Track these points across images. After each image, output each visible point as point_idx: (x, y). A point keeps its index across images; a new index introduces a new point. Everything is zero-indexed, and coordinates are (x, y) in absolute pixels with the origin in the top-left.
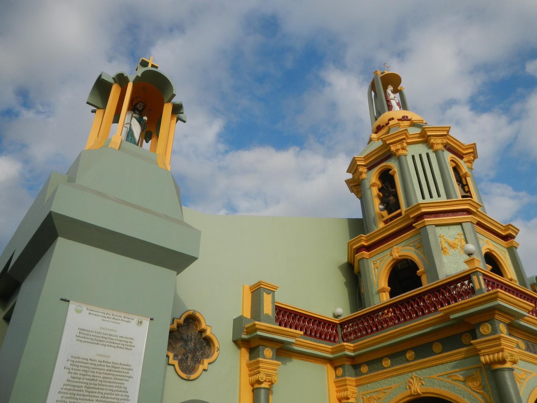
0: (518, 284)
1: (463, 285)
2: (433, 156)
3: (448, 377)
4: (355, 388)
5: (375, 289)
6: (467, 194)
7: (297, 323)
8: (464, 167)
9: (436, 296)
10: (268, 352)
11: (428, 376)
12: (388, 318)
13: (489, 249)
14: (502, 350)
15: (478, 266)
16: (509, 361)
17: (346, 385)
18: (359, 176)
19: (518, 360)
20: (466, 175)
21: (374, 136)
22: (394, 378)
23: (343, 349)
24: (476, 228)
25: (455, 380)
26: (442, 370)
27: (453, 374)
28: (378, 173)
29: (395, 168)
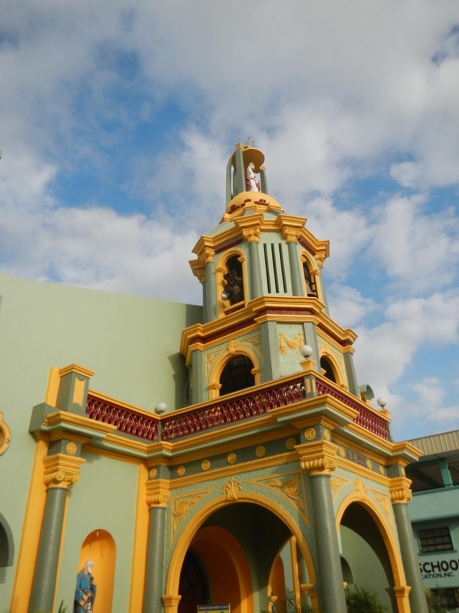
0: (348, 391)
1: (295, 387)
2: (285, 248)
3: (267, 482)
4: (168, 491)
5: (205, 385)
6: (313, 293)
7: (111, 416)
8: (315, 265)
9: (267, 398)
10: (72, 447)
11: (246, 481)
12: (214, 417)
13: (326, 353)
14: (322, 457)
15: (313, 369)
16: (328, 468)
17: (158, 488)
18: (205, 258)
19: (336, 467)
20: (315, 273)
21: (227, 216)
22: (212, 482)
23: (161, 448)
24: (316, 329)
25: (273, 486)
26: (262, 475)
27: (272, 479)
28: (226, 258)
29: (245, 255)
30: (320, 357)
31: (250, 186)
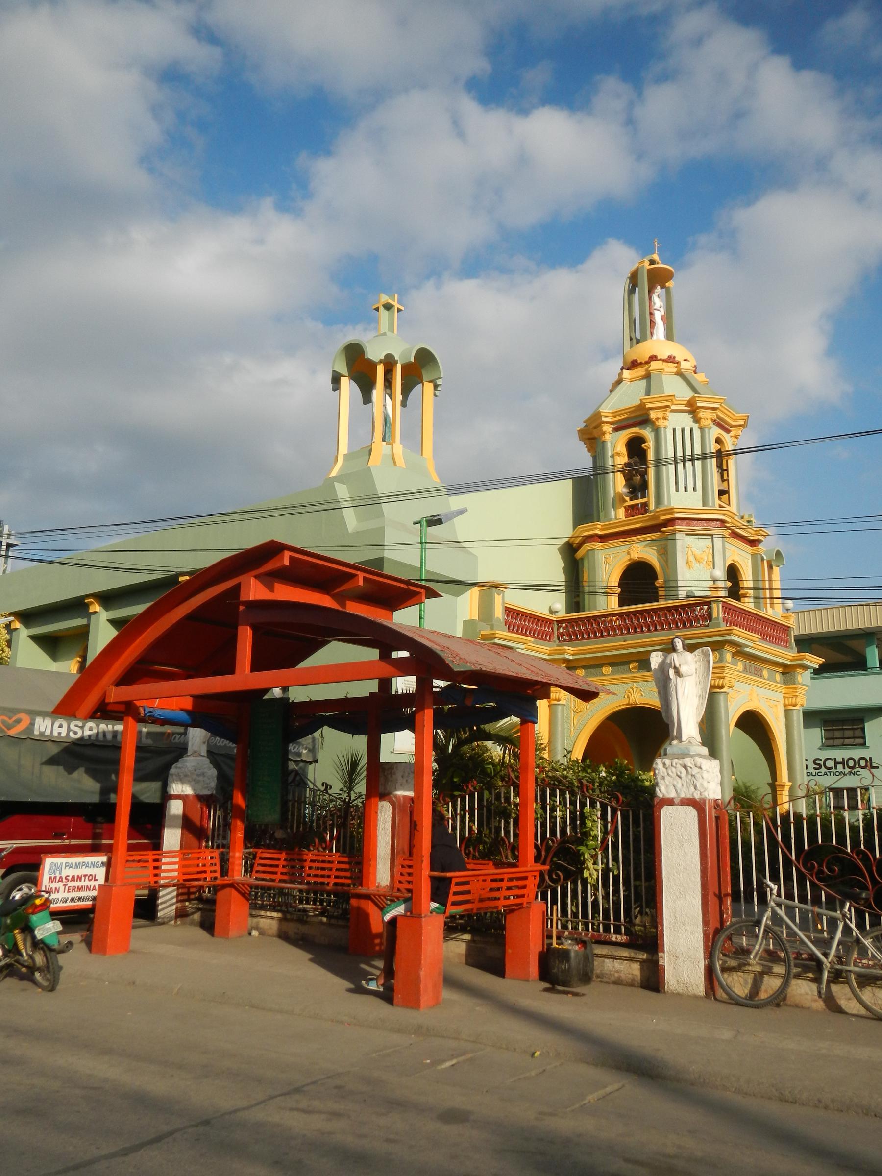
2: (697, 434)
11: (649, 689)
13: (733, 560)
14: (724, 678)
30: (727, 565)
31: (655, 323)
